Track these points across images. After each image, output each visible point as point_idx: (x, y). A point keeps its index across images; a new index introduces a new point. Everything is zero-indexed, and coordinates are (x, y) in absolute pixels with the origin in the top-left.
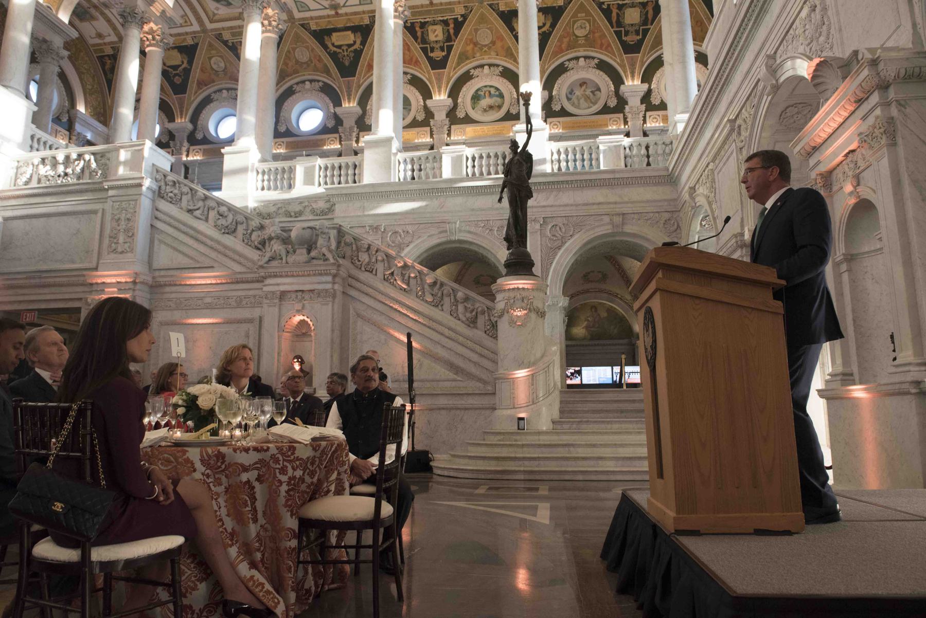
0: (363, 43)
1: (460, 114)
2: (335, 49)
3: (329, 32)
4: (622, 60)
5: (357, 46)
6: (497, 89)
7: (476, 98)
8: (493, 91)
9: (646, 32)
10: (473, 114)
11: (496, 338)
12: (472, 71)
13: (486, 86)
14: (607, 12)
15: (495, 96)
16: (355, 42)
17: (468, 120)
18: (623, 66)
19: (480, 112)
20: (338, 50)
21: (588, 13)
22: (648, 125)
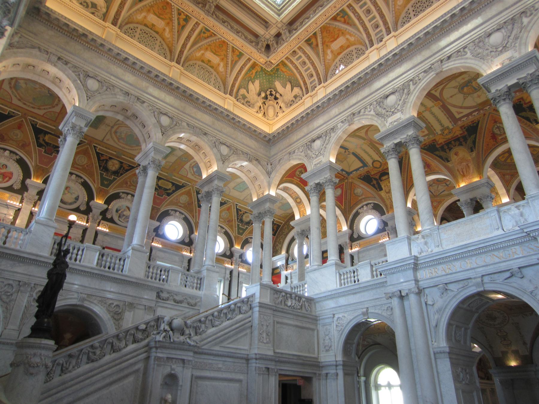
1: (109, 216)
3: (46, 133)
10: (116, 219)
12: (121, 194)
17: (111, 220)
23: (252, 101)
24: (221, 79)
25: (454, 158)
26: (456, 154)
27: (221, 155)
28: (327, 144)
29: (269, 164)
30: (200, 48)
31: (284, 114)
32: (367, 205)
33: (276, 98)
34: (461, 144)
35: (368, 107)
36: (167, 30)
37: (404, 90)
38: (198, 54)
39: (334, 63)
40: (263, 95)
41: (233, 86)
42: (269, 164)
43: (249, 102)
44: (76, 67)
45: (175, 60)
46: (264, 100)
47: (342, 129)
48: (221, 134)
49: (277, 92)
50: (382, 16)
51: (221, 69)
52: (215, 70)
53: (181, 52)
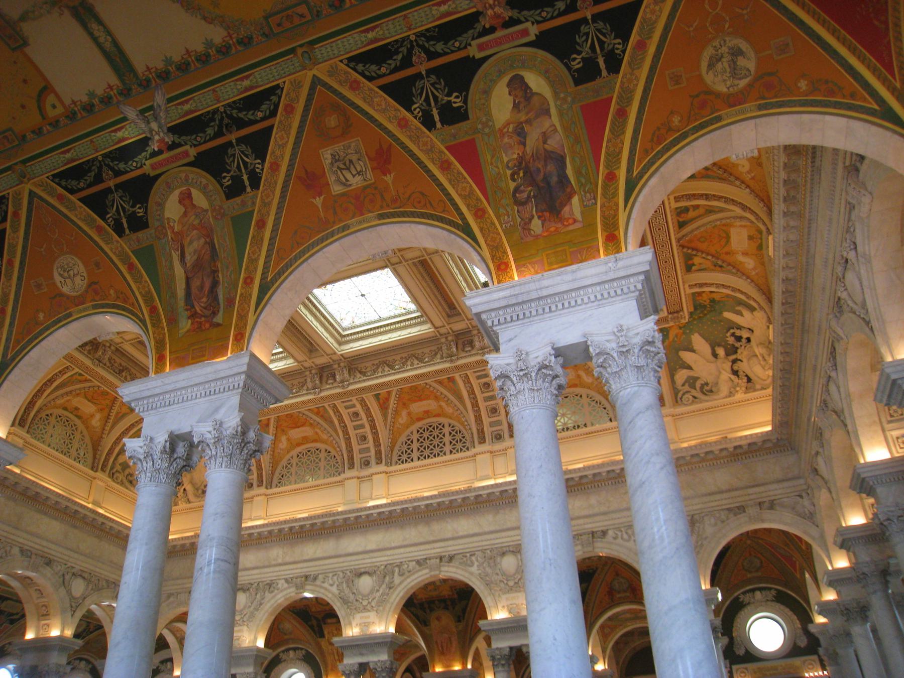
24: (91, 438)
25: (434, 624)
26: (438, 619)
27: (72, 598)
28: (257, 609)
31: (189, 506)
32: (295, 649)
34: (446, 608)
35: (331, 575)
37: (385, 577)
39: (288, 456)
47: (285, 593)
48: (76, 556)
50: (373, 427)
51: (96, 422)
52: (83, 422)
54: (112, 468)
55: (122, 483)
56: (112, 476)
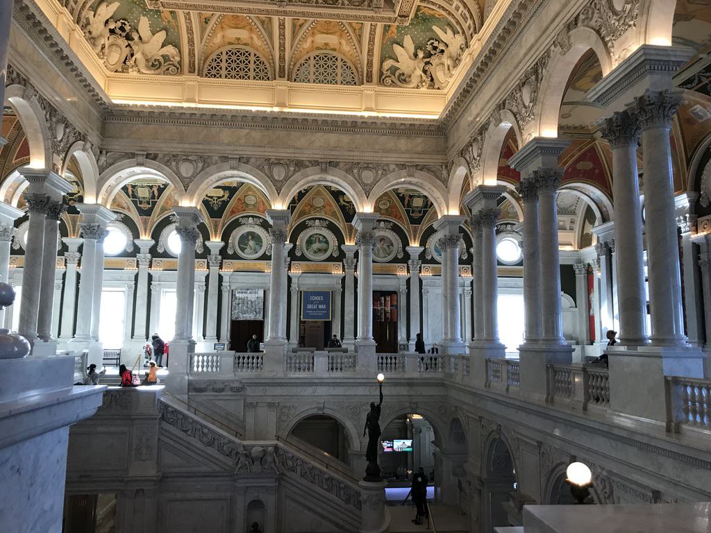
0: (230, 197)
1: (298, 254)
2: (208, 198)
4: (409, 228)
5: (225, 198)
6: (324, 237)
7: (309, 242)
8: (321, 238)
9: (425, 212)
11: (361, 509)
13: (316, 234)
14: (402, 199)
15: (322, 242)
16: (223, 196)
17: (303, 258)
18: (409, 232)
19: (312, 253)
20: (210, 199)
21: (390, 197)
22: (423, 274)
23: (407, 71)
29: (444, 167)
30: (304, 39)
33: (442, 51)
36: (255, 37)
38: (307, 45)
40: (421, 54)
41: (370, 64)
42: (444, 167)
43: (403, 74)
44: (165, 155)
45: (277, 76)
46: (428, 60)
49: (439, 41)
53: (282, 58)
54: (380, 77)
55: (393, 84)
56: (381, 82)
